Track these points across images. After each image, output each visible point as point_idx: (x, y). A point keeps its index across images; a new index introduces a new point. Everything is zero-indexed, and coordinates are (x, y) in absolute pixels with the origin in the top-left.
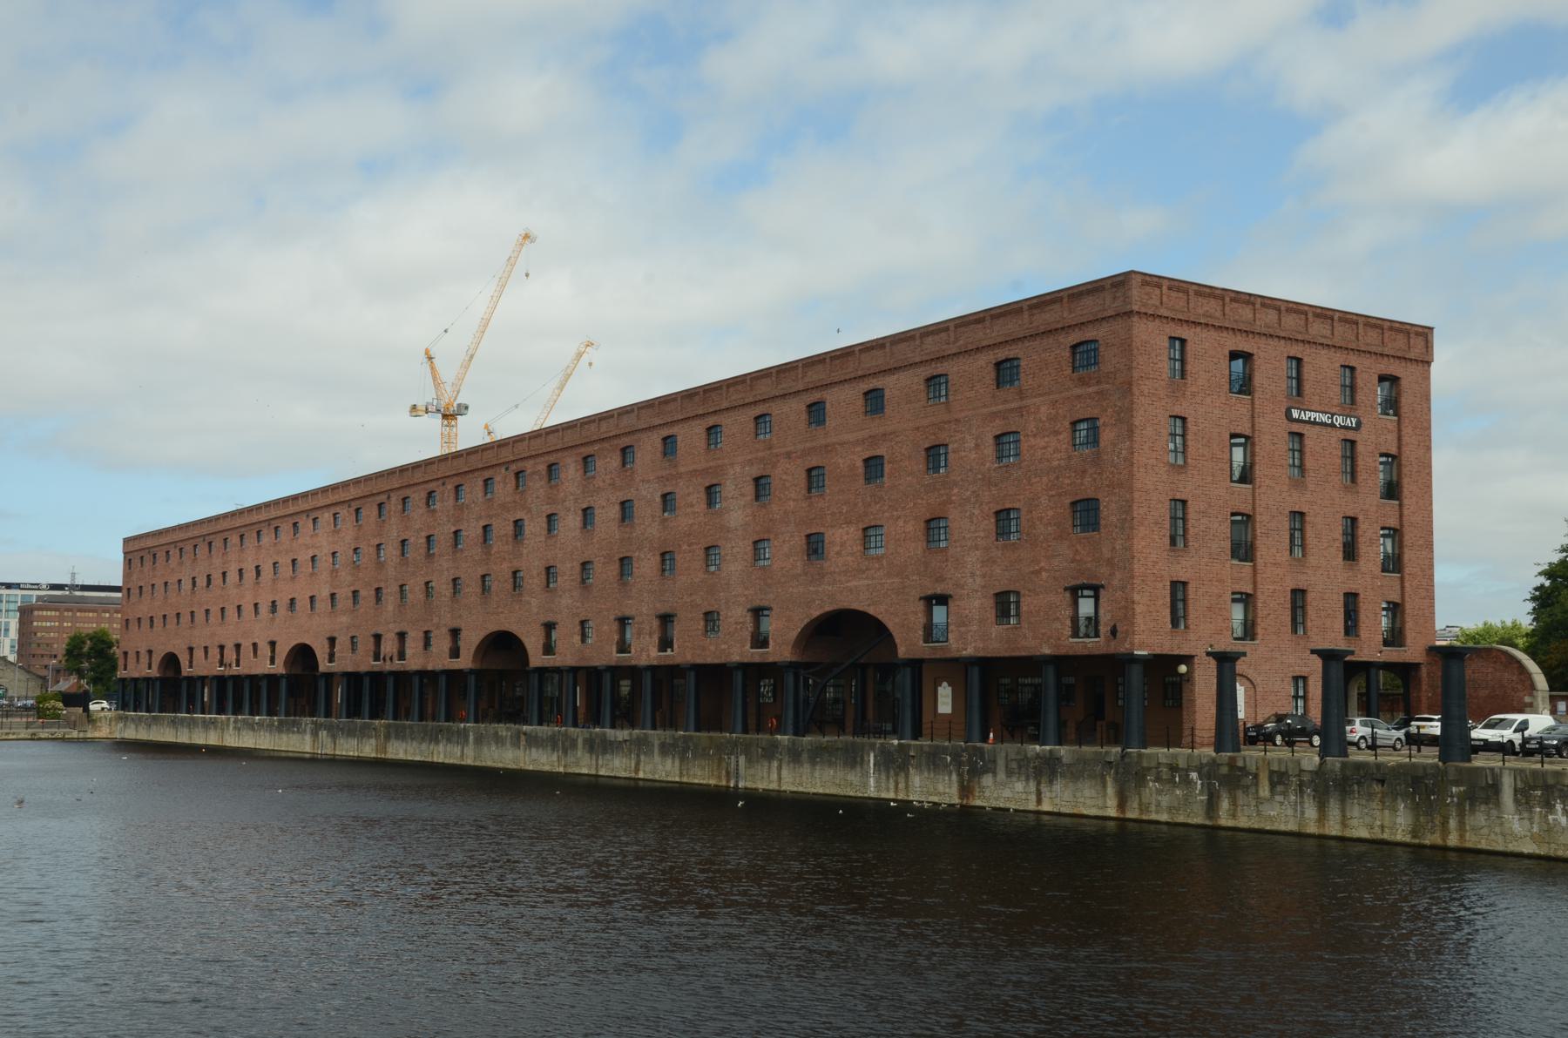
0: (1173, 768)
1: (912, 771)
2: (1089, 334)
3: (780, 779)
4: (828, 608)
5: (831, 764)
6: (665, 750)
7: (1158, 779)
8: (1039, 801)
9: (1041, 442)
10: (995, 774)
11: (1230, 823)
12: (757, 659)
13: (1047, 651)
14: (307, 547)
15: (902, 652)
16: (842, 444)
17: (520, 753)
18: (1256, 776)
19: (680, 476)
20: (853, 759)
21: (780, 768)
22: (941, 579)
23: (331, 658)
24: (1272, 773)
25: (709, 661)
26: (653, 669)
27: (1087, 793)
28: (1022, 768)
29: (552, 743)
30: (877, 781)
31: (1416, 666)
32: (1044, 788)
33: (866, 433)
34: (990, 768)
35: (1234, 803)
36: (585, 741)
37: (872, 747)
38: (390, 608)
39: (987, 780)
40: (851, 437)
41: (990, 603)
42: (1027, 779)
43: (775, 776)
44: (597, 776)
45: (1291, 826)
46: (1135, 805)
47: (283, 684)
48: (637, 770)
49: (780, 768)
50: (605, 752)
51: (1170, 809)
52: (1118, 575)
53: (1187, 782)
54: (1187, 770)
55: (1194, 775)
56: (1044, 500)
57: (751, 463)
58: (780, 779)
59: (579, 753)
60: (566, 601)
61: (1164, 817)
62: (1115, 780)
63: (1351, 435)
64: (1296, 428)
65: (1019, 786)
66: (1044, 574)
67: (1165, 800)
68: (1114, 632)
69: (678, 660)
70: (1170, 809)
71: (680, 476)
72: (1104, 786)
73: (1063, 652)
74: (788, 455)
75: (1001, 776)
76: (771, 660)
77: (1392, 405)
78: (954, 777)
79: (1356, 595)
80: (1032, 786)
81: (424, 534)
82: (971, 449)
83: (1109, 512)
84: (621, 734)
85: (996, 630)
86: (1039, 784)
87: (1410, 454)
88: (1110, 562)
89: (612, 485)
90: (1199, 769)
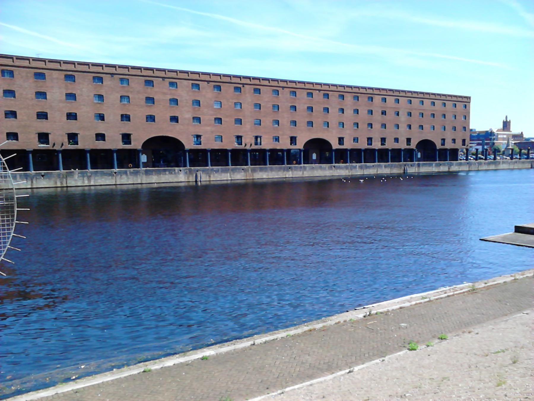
6: (385, 167)
15: (438, 148)
17: (331, 171)
20: (431, 165)
29: (347, 168)
34: (453, 165)
36: (359, 167)
48: (377, 171)
60: (348, 132)
71: (387, 107)
79: (343, 138)
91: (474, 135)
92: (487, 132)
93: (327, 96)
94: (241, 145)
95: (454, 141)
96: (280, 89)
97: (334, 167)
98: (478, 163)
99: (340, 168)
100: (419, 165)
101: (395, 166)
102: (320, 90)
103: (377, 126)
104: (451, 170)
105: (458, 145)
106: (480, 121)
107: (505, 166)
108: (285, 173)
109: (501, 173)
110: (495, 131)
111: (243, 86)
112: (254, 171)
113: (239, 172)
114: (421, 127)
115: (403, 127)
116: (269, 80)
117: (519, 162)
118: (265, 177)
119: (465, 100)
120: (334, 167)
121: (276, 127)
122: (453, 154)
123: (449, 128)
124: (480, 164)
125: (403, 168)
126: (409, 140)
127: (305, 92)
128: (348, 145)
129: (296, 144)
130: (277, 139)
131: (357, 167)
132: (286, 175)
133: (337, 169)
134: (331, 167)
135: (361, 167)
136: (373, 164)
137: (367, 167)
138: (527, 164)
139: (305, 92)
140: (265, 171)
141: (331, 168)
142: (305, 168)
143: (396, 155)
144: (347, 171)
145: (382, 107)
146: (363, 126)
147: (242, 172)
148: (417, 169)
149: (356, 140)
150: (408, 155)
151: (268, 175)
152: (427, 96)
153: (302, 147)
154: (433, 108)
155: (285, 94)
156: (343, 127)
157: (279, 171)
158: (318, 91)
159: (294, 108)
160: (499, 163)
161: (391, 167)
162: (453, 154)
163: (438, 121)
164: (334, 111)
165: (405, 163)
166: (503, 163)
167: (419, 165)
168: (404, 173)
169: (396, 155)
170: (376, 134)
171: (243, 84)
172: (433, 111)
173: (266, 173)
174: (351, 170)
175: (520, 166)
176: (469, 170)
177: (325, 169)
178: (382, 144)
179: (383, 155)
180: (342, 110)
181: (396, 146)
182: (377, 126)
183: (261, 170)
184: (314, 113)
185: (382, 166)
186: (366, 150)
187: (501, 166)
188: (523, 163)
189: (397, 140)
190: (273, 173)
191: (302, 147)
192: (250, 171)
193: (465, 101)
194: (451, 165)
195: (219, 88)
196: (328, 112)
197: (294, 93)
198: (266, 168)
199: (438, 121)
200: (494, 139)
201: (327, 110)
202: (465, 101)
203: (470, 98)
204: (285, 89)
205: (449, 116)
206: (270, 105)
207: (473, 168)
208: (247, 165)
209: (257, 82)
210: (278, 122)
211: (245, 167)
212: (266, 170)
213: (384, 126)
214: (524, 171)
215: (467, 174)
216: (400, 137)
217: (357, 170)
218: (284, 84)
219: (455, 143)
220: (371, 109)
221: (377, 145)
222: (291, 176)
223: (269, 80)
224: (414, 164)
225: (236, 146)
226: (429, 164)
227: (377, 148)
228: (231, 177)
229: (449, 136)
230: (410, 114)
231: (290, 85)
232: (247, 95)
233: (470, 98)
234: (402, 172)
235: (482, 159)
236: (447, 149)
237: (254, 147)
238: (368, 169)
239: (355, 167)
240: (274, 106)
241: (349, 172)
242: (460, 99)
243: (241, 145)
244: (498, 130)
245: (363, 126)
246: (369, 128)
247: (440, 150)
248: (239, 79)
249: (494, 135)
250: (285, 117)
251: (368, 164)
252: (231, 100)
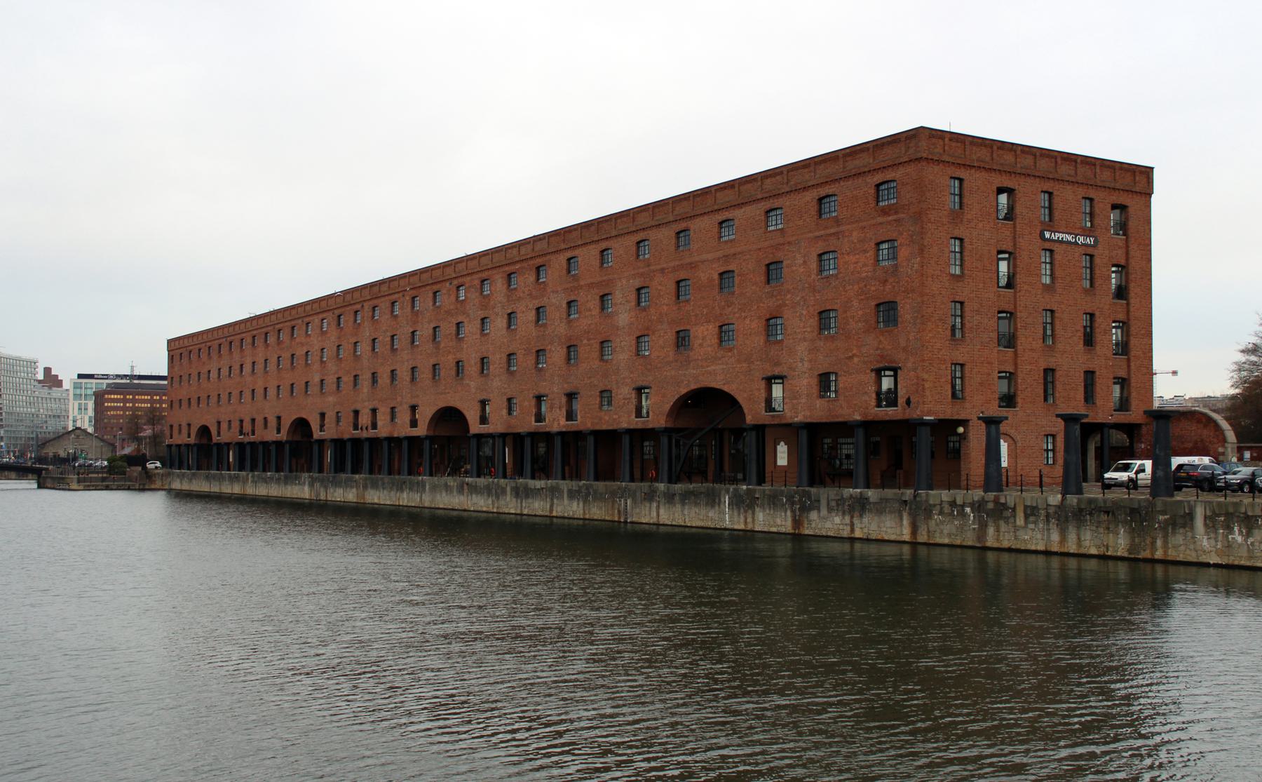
0: (953, 504)
1: (757, 509)
2: (889, 175)
3: (658, 515)
4: (693, 386)
5: (696, 504)
6: (572, 495)
7: (941, 513)
8: (852, 530)
9: (853, 258)
10: (819, 510)
11: (996, 545)
12: (640, 426)
13: (858, 417)
14: (302, 345)
15: (749, 419)
16: (703, 262)
17: (462, 498)
18: (1014, 509)
19: (581, 287)
20: (712, 500)
21: (658, 508)
22: (778, 364)
23: (219, 434)
24: (1026, 507)
25: (604, 427)
26: (561, 434)
27: (888, 524)
28: (840, 506)
29: (488, 490)
30: (730, 517)
31: (1138, 426)
32: (856, 521)
33: (720, 254)
34: (815, 505)
35: (998, 530)
36: (512, 489)
37: (727, 491)
38: (365, 390)
39: (814, 515)
40: (710, 256)
41: (815, 381)
42: (844, 514)
44: (522, 515)
45: (1041, 547)
46: (924, 533)
47: (287, 447)
49: (658, 508)
50: (527, 497)
51: (949, 535)
52: (912, 359)
53: (962, 514)
54: (963, 506)
55: (968, 510)
56: (855, 303)
58: (658, 515)
60: (496, 383)
61: (946, 541)
62: (909, 514)
63: (1090, 251)
64: (1047, 245)
65: (837, 520)
66: (856, 360)
67: (947, 528)
68: (908, 402)
69: (581, 428)
70: (949, 535)
71: (581, 287)
72: (901, 519)
73: (870, 418)
74: (662, 270)
75: (824, 512)
76: (650, 426)
77: (1123, 227)
78: (789, 513)
79: (1093, 373)
80: (847, 519)
81: (389, 334)
82: (799, 264)
83: (906, 311)
84: (539, 484)
85: (819, 403)
86: (852, 517)
87: (1133, 263)
88: (905, 349)
89: (530, 295)
90: (972, 505)
101: (598, 497)
113: (352, 487)
157: (391, 489)
189: (606, 395)
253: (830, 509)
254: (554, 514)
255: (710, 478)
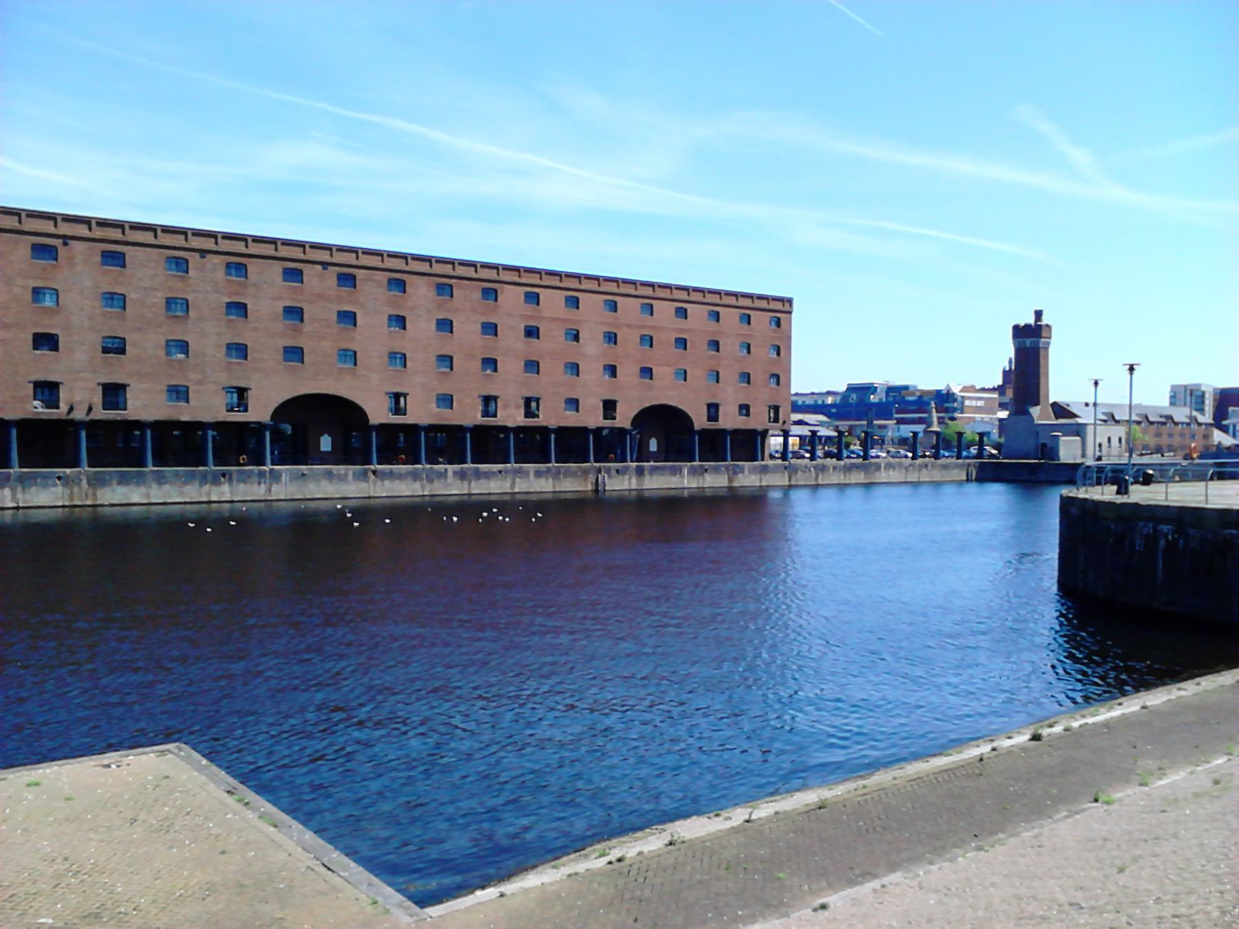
6: (538, 474)
15: (697, 427)
17: (364, 485)
20: (676, 471)
22: (714, 396)
28: (753, 471)
29: (415, 476)
34: (742, 471)
36: (455, 473)
39: (740, 476)
43: (626, 482)
44: (470, 495)
48: (513, 484)
50: (702, 474)
57: (602, 323)
59: (449, 481)
71: (543, 318)
91: (911, 398)
92: (938, 392)
93: (347, 280)
94: (58, 408)
95: (745, 409)
96: (194, 259)
97: (374, 472)
98: (815, 467)
99: (391, 475)
100: (640, 472)
102: (325, 265)
103: (511, 367)
104: (736, 484)
105: (758, 420)
106: (820, 365)
107: (895, 476)
108: (206, 488)
109: (879, 492)
110: (956, 390)
111: (65, 244)
112: (97, 482)
113: (45, 486)
114: (647, 372)
115: (592, 373)
116: (382, 255)
117: (933, 465)
118: (136, 498)
119: (779, 306)
120: (374, 472)
121: (180, 361)
122: (748, 445)
123: (729, 376)
124: (823, 469)
125: (592, 478)
126: (609, 407)
127: (277, 268)
128: (421, 412)
129: (246, 410)
130: (179, 393)
131: (450, 473)
132: (209, 494)
133: (383, 480)
134: (365, 473)
135: (462, 475)
136: (500, 466)
137: (479, 475)
138: (956, 471)
139: (277, 268)
140: (138, 484)
141: (363, 476)
142: (275, 477)
143: (572, 445)
144: (417, 485)
145: (525, 317)
146: (466, 366)
147: (56, 485)
148: (634, 481)
149: (446, 400)
150: (606, 445)
151: (148, 496)
152: (665, 294)
153: (265, 417)
154: (681, 323)
155: (468, 296)
156: (405, 366)
157: (186, 483)
158: (319, 267)
159: (239, 309)
160: (878, 467)
161: (556, 475)
162: (748, 445)
163: (697, 360)
164: (422, 327)
165: (597, 465)
166: (889, 466)
167: (640, 472)
168: (597, 491)
169: (572, 445)
170: (510, 389)
171: (66, 239)
172: (681, 330)
173: (143, 490)
174: (431, 481)
175: (937, 475)
176: (790, 486)
177: (342, 478)
178: (486, 413)
179: (534, 444)
180: (401, 321)
181: (571, 419)
182: (511, 367)
183: (123, 480)
184: (307, 327)
185: (527, 473)
186: (478, 430)
187: (883, 476)
188: (945, 467)
189: (574, 403)
190: (167, 487)
191: (265, 417)
192: (84, 482)
193: (778, 310)
194: (736, 472)
195: (181, 265)
196: (355, 325)
197: (241, 269)
198: (141, 476)
199: (697, 360)
200: (955, 410)
201: (349, 318)
202: (778, 310)
203: (790, 301)
204: (209, 256)
205: (730, 346)
206: (159, 298)
207: (800, 479)
208: (75, 463)
209: (116, 234)
210: (184, 347)
211: (68, 471)
212: (140, 480)
213: (532, 366)
214: (949, 490)
215: (786, 494)
216: (579, 396)
217: (449, 483)
218: (209, 244)
219: (748, 414)
220: (493, 320)
221: (511, 416)
222: (227, 497)
223: (382, 255)
224: (627, 468)
225: (37, 409)
226: (672, 467)
227: (510, 424)
228: (14, 498)
229: (729, 397)
230: (612, 338)
231: (225, 246)
232: (79, 268)
233: (790, 301)
234: (590, 487)
235: (859, 456)
236: (724, 431)
237: (100, 414)
238: (483, 481)
239: (443, 475)
240: (170, 302)
241: (423, 487)
242: (763, 304)
243: (58, 408)
244: (965, 389)
245: (466, 366)
246: (489, 372)
247: (704, 433)
248: (52, 223)
249: (955, 400)
250: (208, 335)
251: (484, 467)
252: (19, 281)
253: (750, 472)
254: (517, 490)
255: (469, 459)
